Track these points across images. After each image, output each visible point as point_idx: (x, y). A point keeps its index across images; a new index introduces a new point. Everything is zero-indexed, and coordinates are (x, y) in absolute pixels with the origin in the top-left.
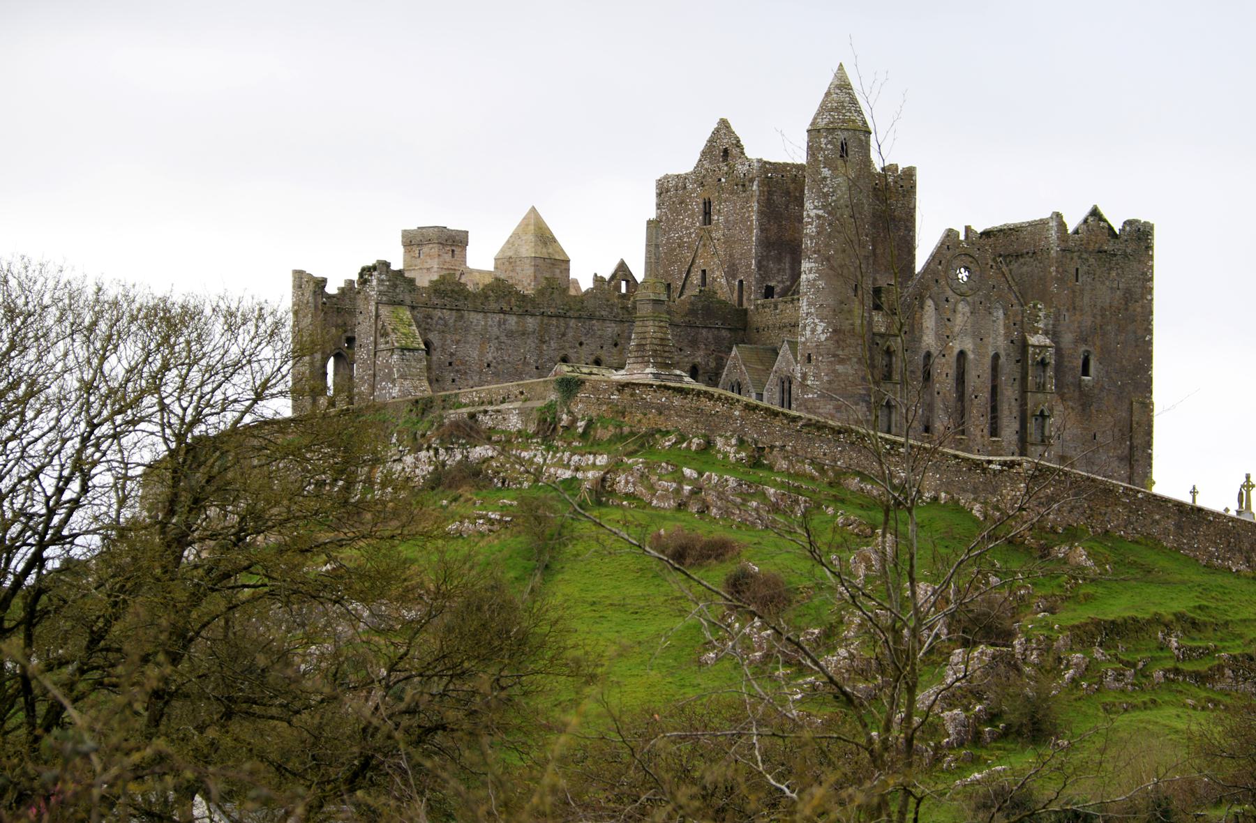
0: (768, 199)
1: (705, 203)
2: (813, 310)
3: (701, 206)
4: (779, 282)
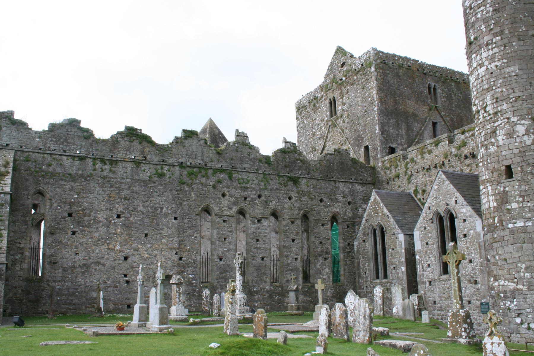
0: (383, 79)
1: (330, 103)
2: (505, 107)
3: (328, 105)
4: (398, 144)
